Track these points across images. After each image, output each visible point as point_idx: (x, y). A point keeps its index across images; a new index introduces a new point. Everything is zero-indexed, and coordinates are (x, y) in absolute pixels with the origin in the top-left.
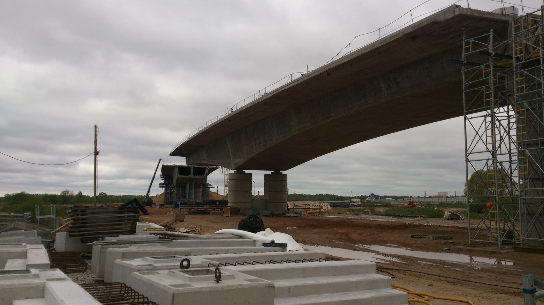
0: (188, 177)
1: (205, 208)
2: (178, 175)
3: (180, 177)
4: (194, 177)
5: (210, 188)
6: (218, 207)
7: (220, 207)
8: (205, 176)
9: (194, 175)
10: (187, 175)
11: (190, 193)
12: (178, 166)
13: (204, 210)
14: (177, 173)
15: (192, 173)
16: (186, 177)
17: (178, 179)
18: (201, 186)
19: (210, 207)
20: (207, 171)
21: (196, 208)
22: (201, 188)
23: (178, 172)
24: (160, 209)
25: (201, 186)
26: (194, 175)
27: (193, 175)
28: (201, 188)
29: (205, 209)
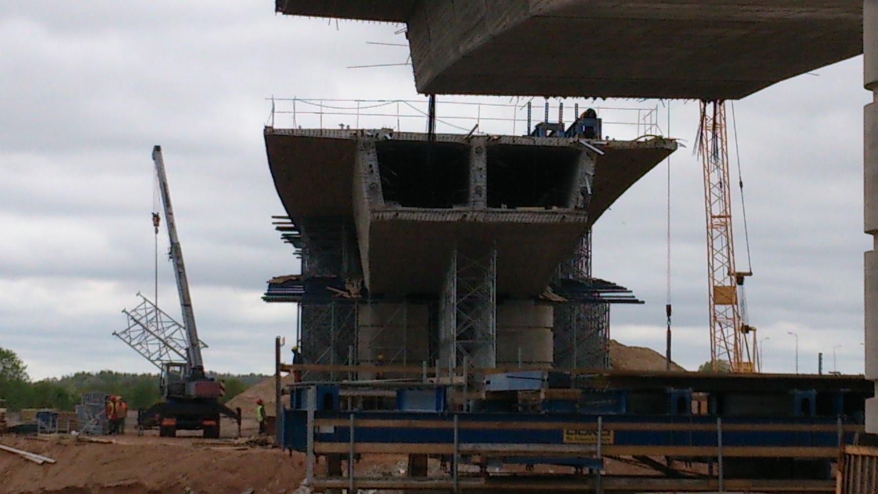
0: (451, 215)
1: (570, 447)
2: (381, 203)
3: (388, 216)
4: (492, 219)
5: (613, 307)
6: (708, 439)
7: (730, 439)
8: (572, 206)
9: (493, 201)
10: (443, 203)
11: (466, 335)
12: (375, 133)
13: (573, 470)
14: (372, 189)
16: (440, 218)
17: (376, 226)
18: (549, 293)
19: (622, 438)
21: (484, 447)
22: (549, 301)
23: (377, 179)
24: (258, 450)
25: (549, 293)
26: (493, 201)
27: (482, 205)
28: (549, 301)
29: (578, 462)
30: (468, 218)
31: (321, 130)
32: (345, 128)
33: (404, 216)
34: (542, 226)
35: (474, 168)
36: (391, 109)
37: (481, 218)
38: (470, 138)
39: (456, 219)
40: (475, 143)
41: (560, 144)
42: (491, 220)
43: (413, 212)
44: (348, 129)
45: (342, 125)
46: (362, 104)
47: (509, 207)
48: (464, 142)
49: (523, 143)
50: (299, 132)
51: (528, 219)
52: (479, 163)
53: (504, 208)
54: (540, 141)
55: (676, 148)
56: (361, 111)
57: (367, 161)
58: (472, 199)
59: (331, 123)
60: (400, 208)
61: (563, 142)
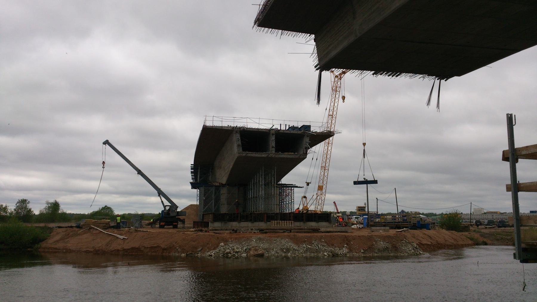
0: (264, 155)
4: (277, 156)
9: (277, 150)
12: (240, 128)
14: (238, 146)
15: (273, 147)
20: (307, 140)
23: (240, 143)
27: (274, 152)
30: (269, 156)
31: (222, 127)
32: (229, 126)
33: (249, 155)
34: (292, 159)
35: (271, 140)
36: (245, 120)
37: (273, 156)
38: (271, 130)
39: (265, 156)
40: (272, 132)
41: (298, 133)
42: (276, 156)
43: (252, 154)
44: (230, 126)
45: (228, 125)
46: (235, 118)
47: (281, 153)
48: (268, 131)
49: (287, 132)
50: (215, 127)
51: (289, 157)
52: (273, 138)
53: (280, 153)
54: (292, 132)
55: (334, 135)
56: (235, 121)
57: (236, 138)
58: (270, 150)
59: (225, 124)
60: (247, 152)
61: (299, 132)
